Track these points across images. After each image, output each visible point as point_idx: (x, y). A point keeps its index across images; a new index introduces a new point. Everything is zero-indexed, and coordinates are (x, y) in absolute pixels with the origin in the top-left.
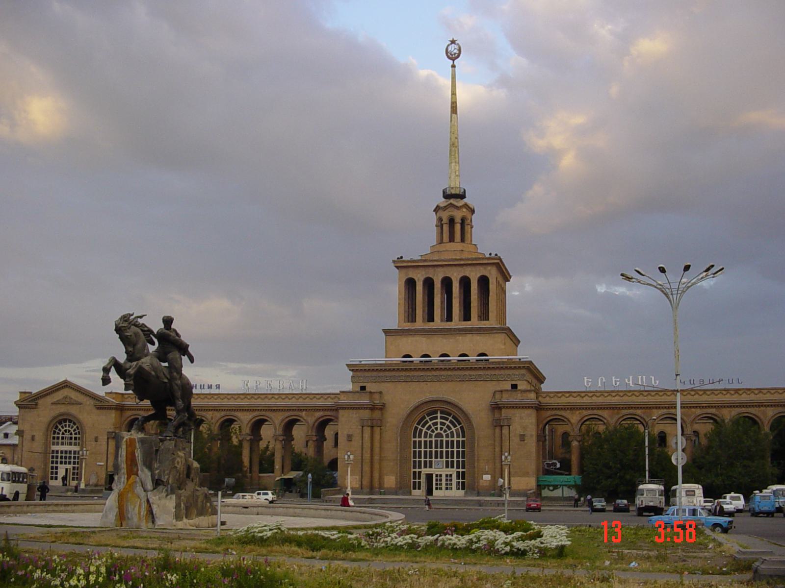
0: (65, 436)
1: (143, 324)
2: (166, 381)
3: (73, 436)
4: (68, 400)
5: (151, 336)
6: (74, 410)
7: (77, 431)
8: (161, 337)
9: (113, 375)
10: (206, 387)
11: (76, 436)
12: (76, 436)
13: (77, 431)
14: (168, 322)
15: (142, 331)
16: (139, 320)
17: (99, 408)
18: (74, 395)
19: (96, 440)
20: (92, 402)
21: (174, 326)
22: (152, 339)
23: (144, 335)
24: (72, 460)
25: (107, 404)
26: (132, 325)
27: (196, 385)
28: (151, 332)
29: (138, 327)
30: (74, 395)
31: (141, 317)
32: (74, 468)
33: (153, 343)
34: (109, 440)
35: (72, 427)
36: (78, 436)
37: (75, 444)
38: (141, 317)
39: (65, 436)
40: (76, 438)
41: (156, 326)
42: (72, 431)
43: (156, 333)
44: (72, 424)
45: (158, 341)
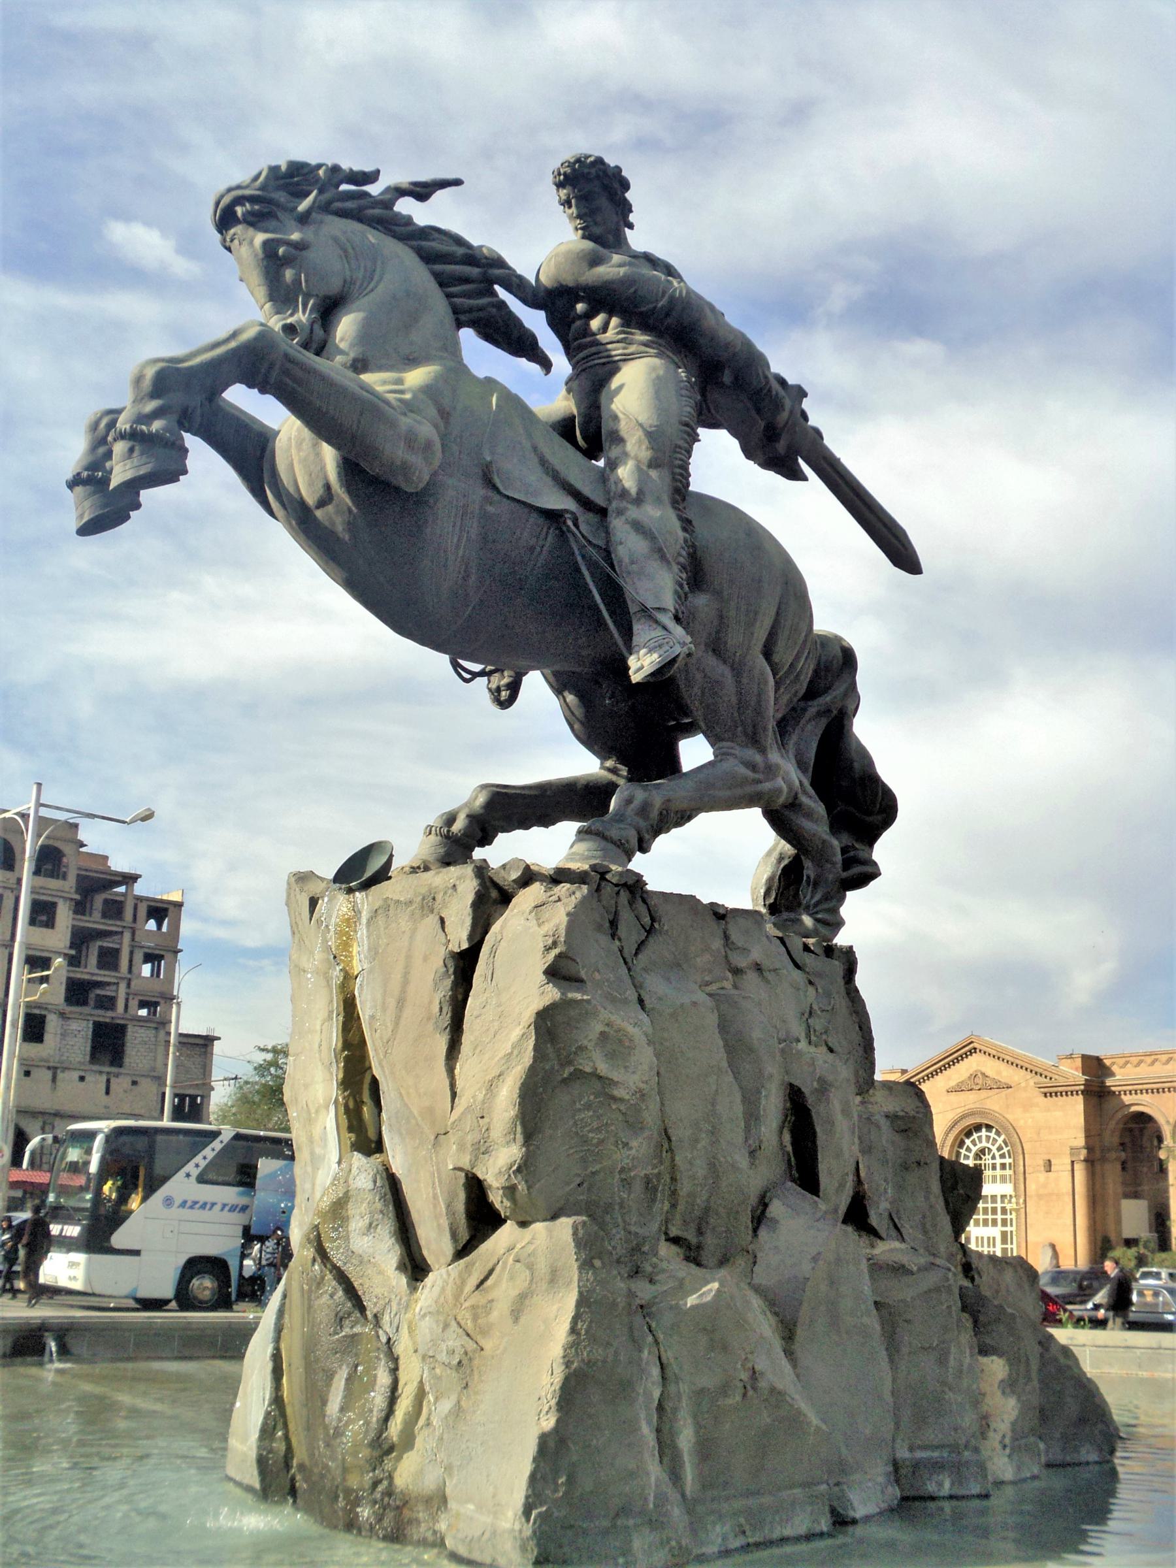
0: (983, 1162)
3: (998, 1161)
4: (979, 1080)
5: (497, 287)
6: (994, 1103)
7: (1005, 1150)
11: (1003, 1161)
12: (1003, 1161)
13: (1005, 1150)
17: (1049, 1093)
18: (991, 1068)
19: (1048, 1166)
20: (1032, 1080)
22: (502, 305)
23: (443, 281)
24: (999, 1217)
25: (1062, 1081)
26: (343, 214)
29: (403, 238)
30: (991, 1068)
31: (422, 191)
32: (1004, 1235)
33: (521, 344)
34: (1076, 1166)
35: (995, 1140)
36: (1007, 1161)
37: (1003, 1179)
38: (422, 191)
39: (983, 1162)
40: (1003, 1166)
42: (994, 1149)
44: (993, 1135)
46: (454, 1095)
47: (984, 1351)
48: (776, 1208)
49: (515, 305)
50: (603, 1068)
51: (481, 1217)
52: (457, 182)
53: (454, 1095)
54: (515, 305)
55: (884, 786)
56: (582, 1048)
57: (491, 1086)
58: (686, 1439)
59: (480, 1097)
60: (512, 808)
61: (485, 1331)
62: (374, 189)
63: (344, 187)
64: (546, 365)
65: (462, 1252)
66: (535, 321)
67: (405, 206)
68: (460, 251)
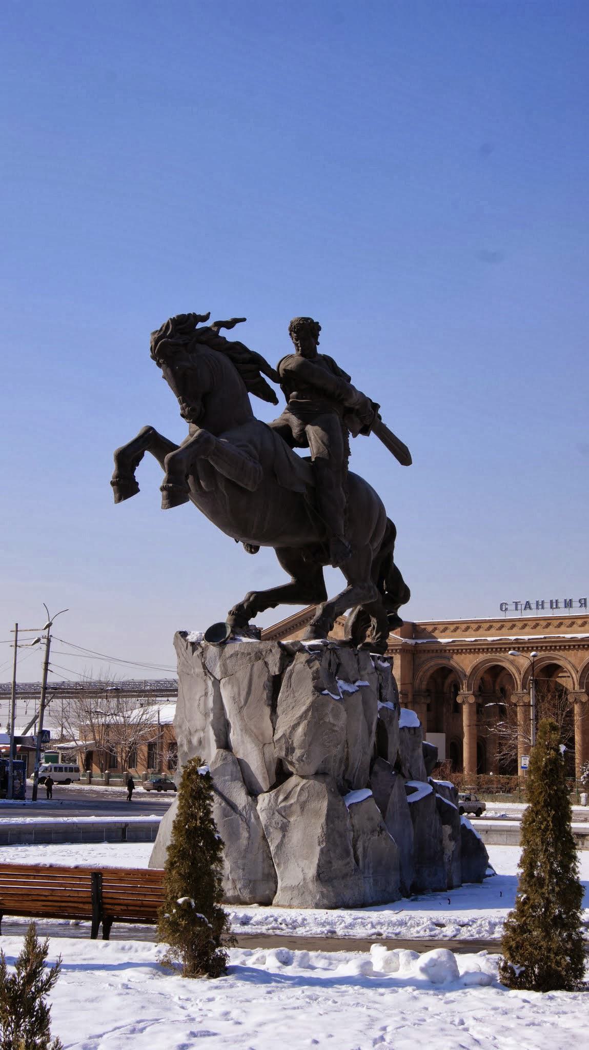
1: (238, 344)
2: (301, 489)
5: (263, 375)
8: (288, 379)
9: (151, 472)
10: (561, 605)
14: (306, 332)
15: (234, 360)
16: (223, 332)
21: (322, 349)
26: (202, 343)
27: (543, 602)
28: (257, 361)
31: (230, 325)
33: (270, 397)
38: (230, 325)
41: (276, 348)
43: (274, 366)
45: (283, 389)
46: (274, 729)
47: (444, 823)
48: (376, 768)
49: (269, 381)
50: (332, 720)
51: (280, 775)
52: (244, 320)
53: (274, 729)
54: (269, 381)
55: (406, 586)
56: (327, 714)
57: (294, 727)
58: (360, 851)
59: (288, 731)
60: (263, 600)
61: (291, 814)
62: (209, 323)
63: (200, 325)
64: (275, 401)
65: (272, 788)
66: (276, 387)
67: (223, 332)
68: (246, 356)
